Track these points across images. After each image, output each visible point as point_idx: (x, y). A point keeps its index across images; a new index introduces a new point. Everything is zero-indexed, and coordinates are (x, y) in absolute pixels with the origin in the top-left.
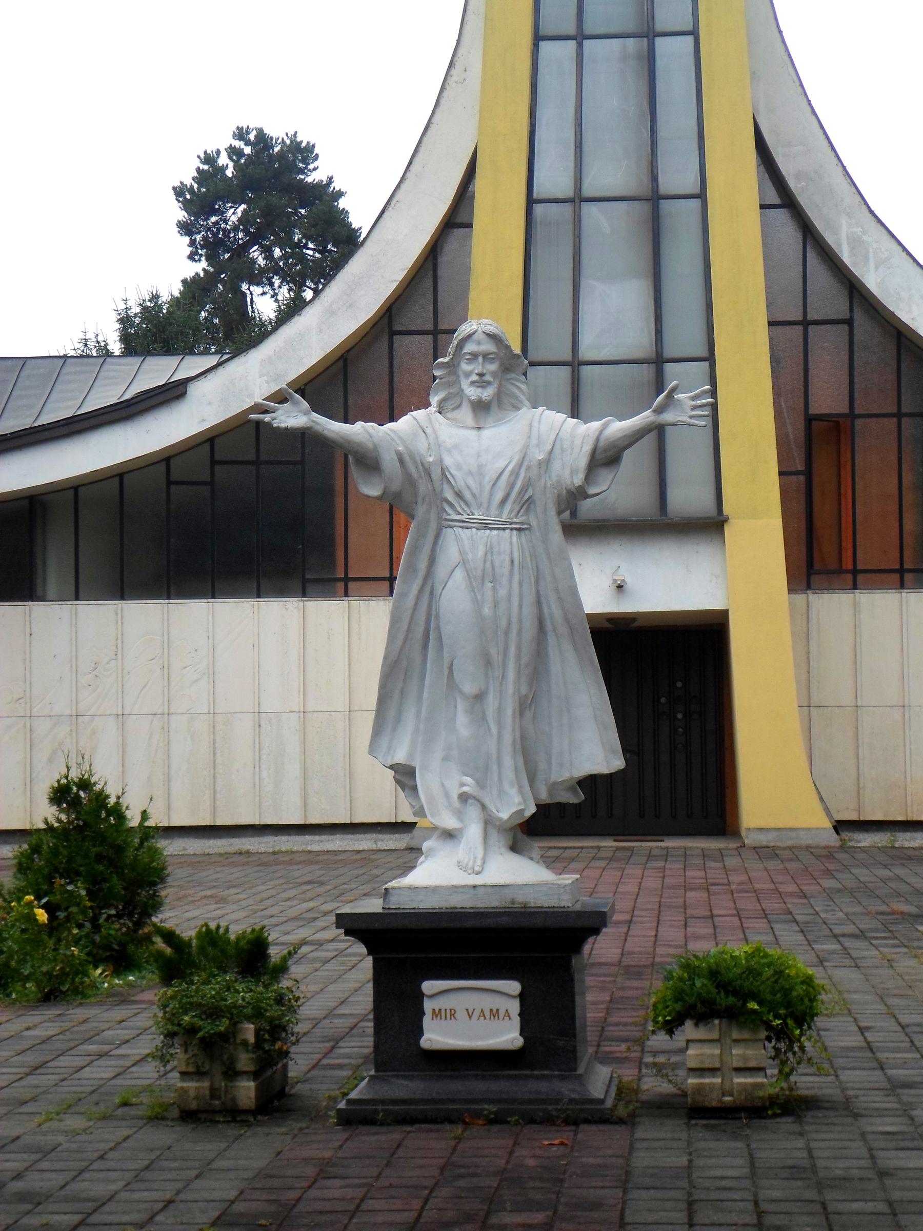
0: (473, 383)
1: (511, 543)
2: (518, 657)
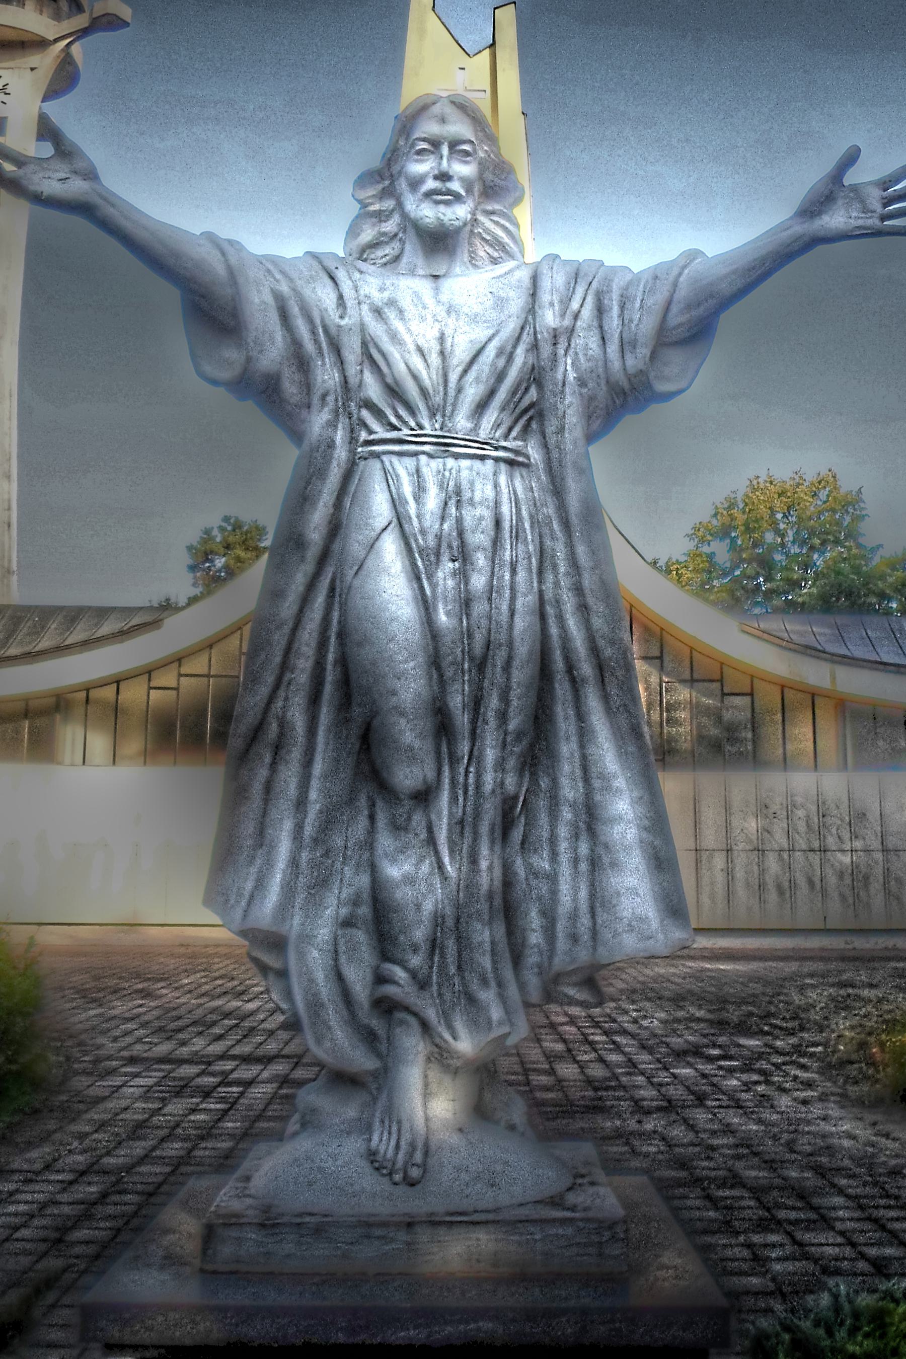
0: (429, 195)
1: (496, 486)
2: (503, 717)
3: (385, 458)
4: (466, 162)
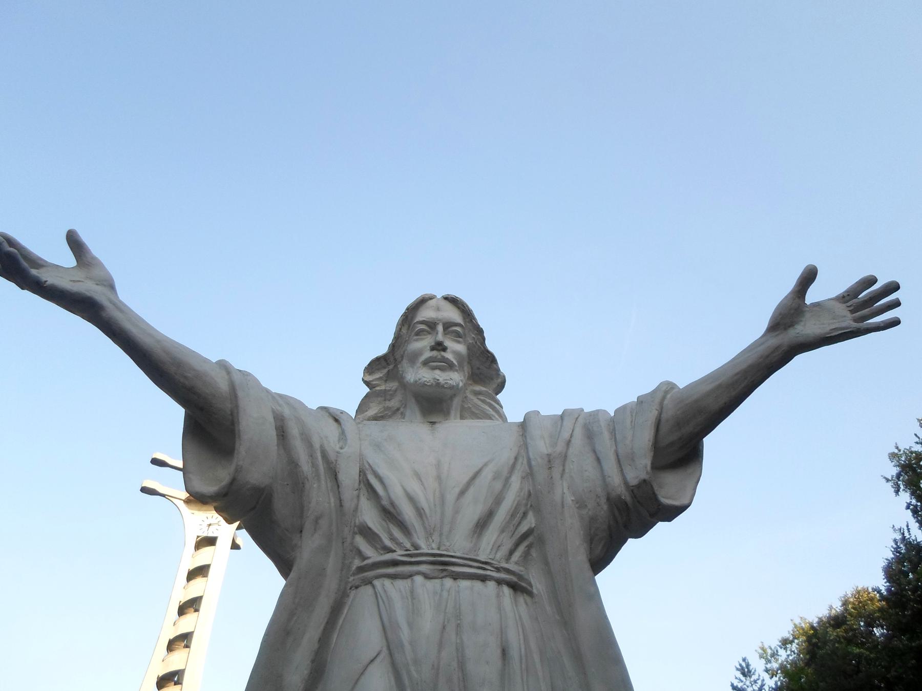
0: (425, 363)
1: (500, 608)
3: (377, 583)
4: (459, 342)
